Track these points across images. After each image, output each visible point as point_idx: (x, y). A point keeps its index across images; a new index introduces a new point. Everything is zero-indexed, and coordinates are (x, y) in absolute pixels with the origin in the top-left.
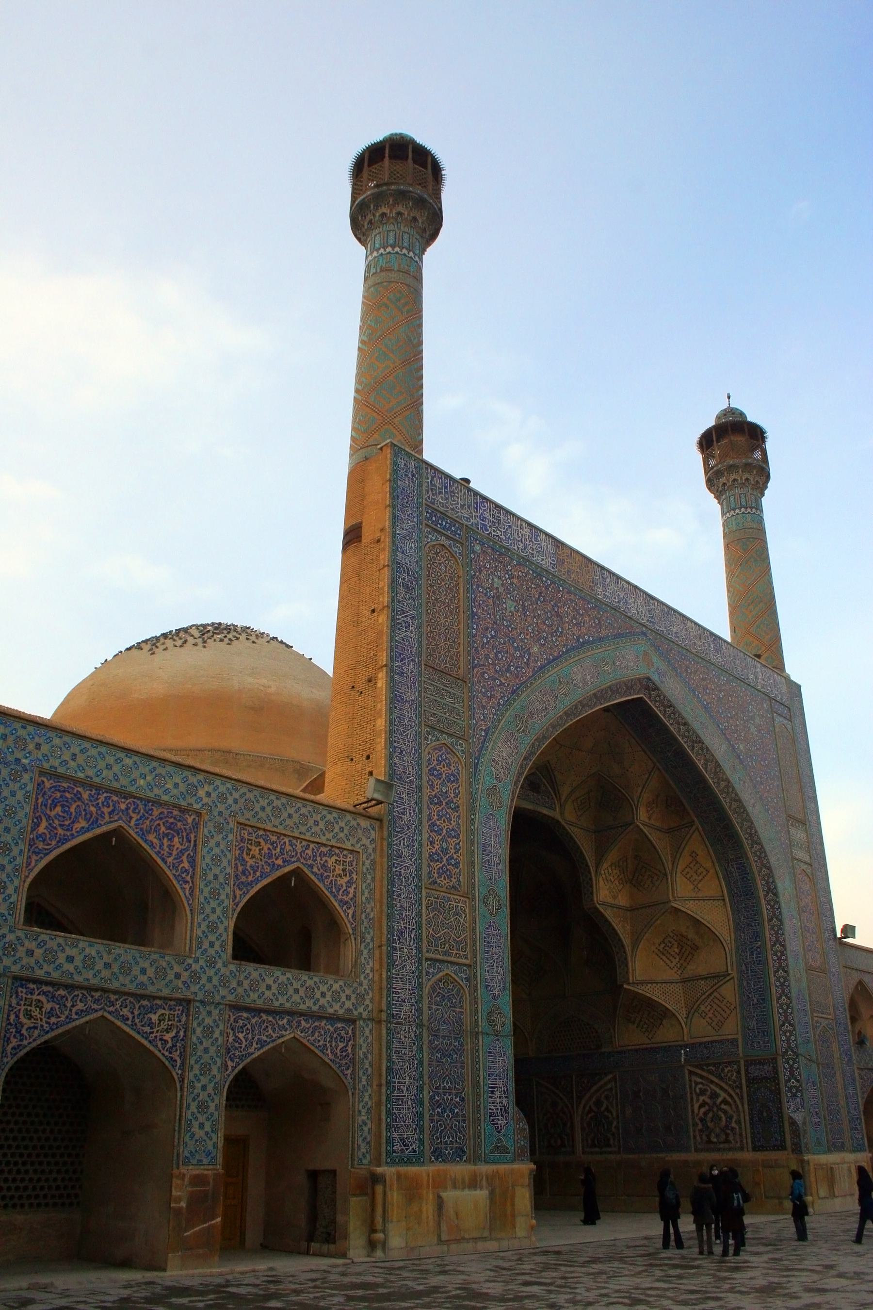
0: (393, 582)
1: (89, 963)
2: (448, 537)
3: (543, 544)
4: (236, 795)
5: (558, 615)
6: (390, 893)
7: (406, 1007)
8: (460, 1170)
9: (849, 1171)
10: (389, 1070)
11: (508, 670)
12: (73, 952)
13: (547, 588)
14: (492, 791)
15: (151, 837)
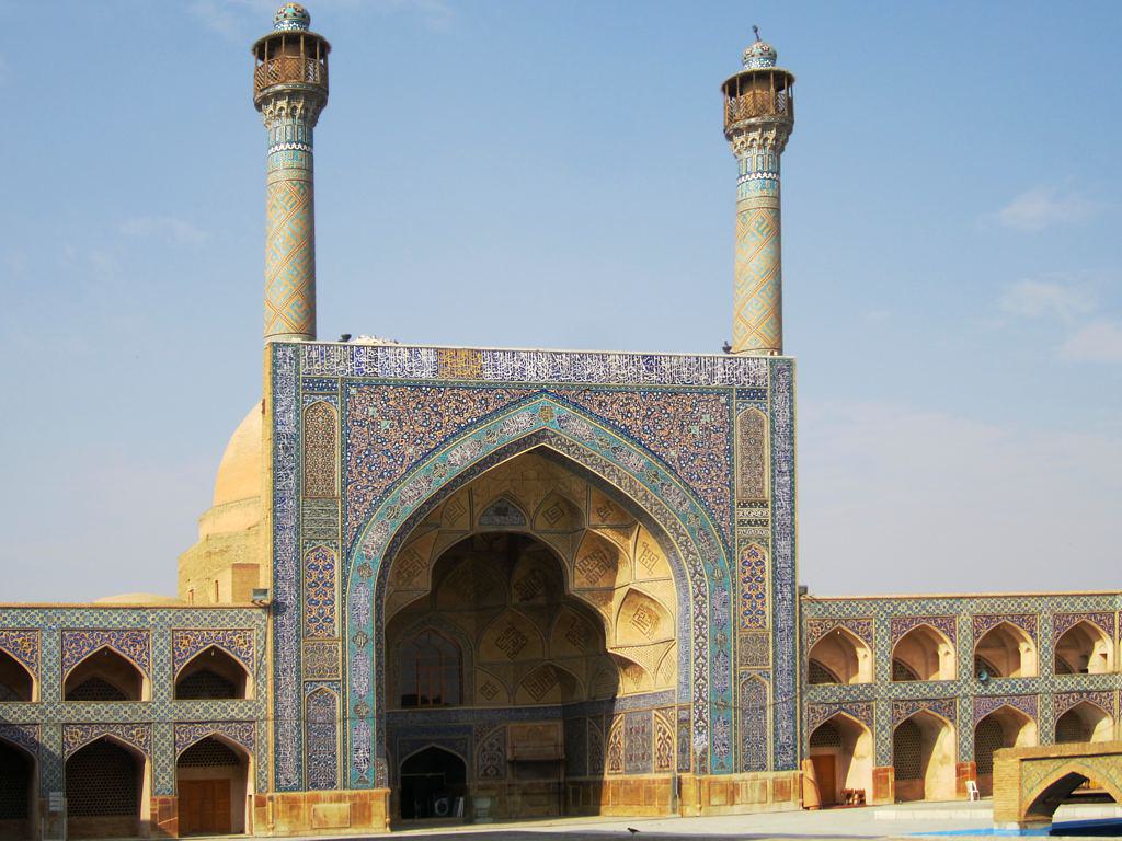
0: (275, 448)
1: (98, 713)
2: (324, 395)
3: (424, 359)
4: (170, 615)
5: (437, 413)
6: (276, 649)
7: (289, 710)
8: (324, 793)
9: (764, 785)
10: (277, 745)
11: (382, 476)
12: (90, 709)
13: (426, 395)
14: (363, 567)
15: (124, 648)
